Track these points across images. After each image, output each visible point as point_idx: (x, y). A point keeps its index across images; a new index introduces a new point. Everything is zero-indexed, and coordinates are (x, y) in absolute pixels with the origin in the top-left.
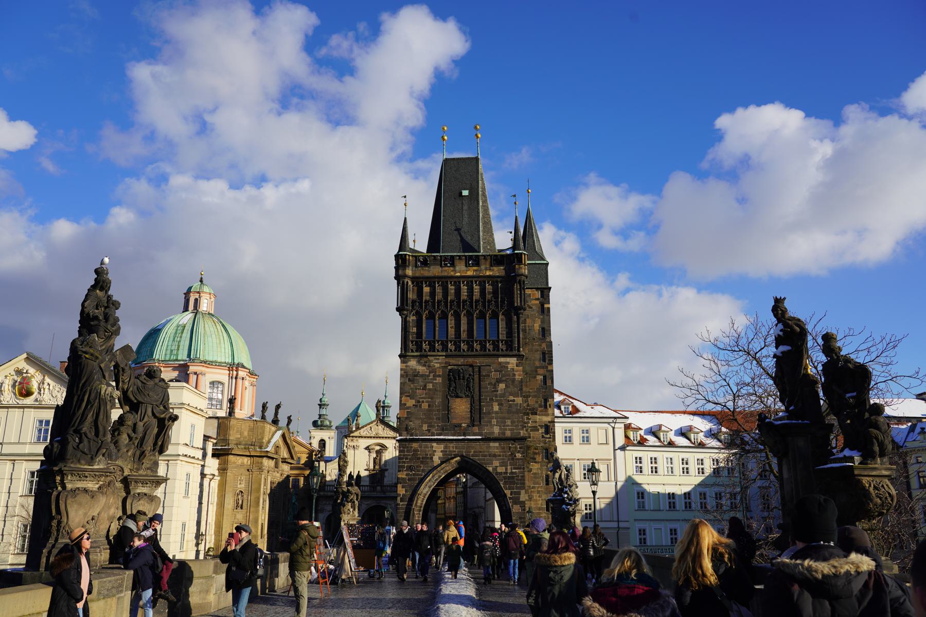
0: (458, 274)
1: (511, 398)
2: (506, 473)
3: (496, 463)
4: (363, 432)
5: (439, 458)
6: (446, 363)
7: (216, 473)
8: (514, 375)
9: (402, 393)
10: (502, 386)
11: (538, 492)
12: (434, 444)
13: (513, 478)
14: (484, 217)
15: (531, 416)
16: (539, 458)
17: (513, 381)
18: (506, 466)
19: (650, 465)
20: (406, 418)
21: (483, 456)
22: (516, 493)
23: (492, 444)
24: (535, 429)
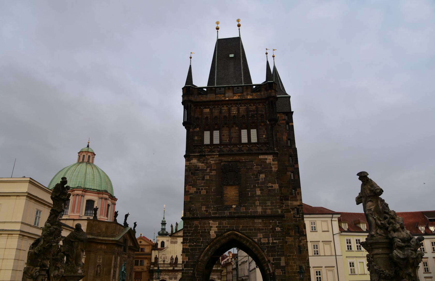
0: (227, 99)
1: (270, 185)
2: (268, 243)
3: (260, 235)
5: (215, 232)
8: (271, 168)
9: (187, 182)
10: (262, 176)
11: (293, 259)
13: (274, 247)
15: (284, 202)
16: (292, 233)
17: (271, 172)
18: (268, 238)
19: (356, 245)
20: (190, 202)
21: (249, 230)
22: (277, 259)
23: (256, 221)
24: (288, 211)
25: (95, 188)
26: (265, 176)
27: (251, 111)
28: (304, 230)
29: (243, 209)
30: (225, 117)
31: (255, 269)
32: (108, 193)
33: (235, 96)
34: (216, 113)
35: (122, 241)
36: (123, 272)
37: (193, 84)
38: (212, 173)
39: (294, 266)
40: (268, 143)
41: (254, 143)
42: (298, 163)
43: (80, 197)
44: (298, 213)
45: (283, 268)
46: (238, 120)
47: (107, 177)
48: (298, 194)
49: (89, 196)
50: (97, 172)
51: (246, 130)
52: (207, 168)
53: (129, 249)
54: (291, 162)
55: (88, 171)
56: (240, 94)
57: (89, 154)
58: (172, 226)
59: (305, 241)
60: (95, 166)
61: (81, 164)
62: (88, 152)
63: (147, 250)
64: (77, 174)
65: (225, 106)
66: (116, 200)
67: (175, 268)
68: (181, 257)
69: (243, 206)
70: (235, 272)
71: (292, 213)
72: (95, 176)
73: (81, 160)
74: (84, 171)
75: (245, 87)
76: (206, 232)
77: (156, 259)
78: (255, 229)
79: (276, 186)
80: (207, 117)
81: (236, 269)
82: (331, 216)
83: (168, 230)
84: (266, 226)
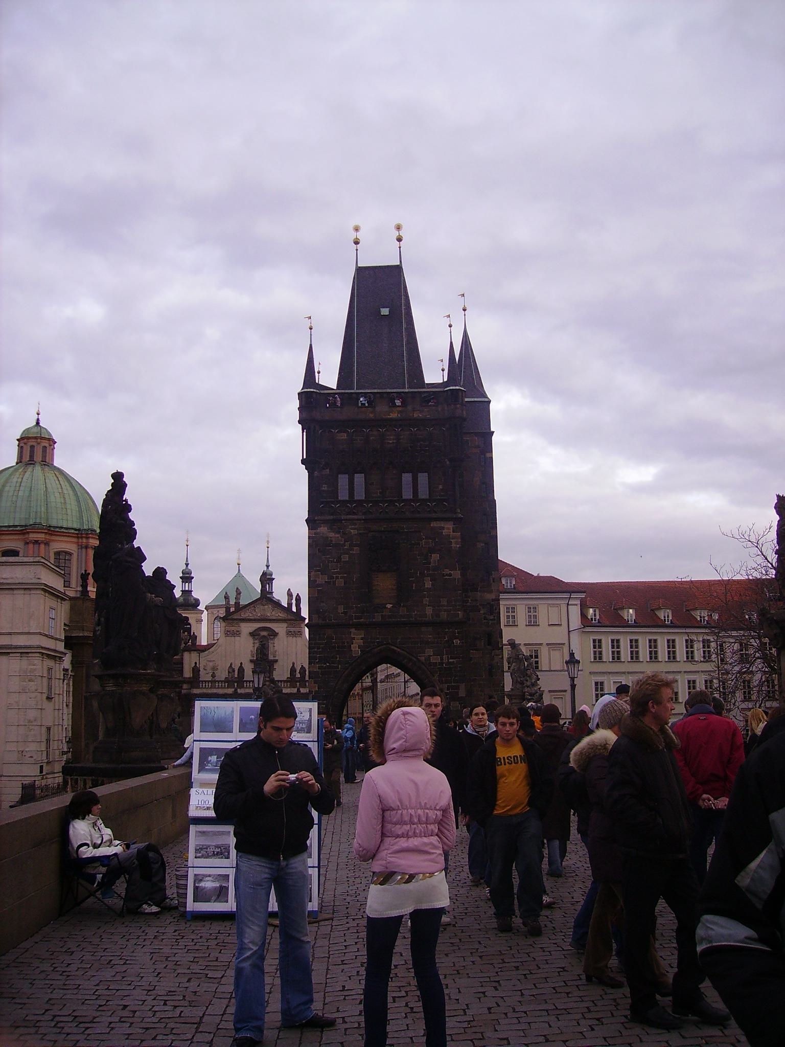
1: (447, 571)
2: (441, 663)
3: (429, 652)
10: (435, 557)
12: (353, 630)
14: (408, 343)
23: (423, 629)
25: (70, 525)
40: (445, 500)
41: (423, 500)
43: (42, 546)
46: (395, 440)
47: (88, 493)
52: (345, 541)
55: (49, 486)
57: (45, 443)
60: (59, 469)
61: (30, 468)
62: (42, 438)
64: (27, 493)
67: (239, 691)
68: (252, 666)
70: (368, 697)
72: (66, 496)
74: (43, 487)
77: (196, 670)
79: (457, 574)
81: (373, 689)
82: (566, 595)
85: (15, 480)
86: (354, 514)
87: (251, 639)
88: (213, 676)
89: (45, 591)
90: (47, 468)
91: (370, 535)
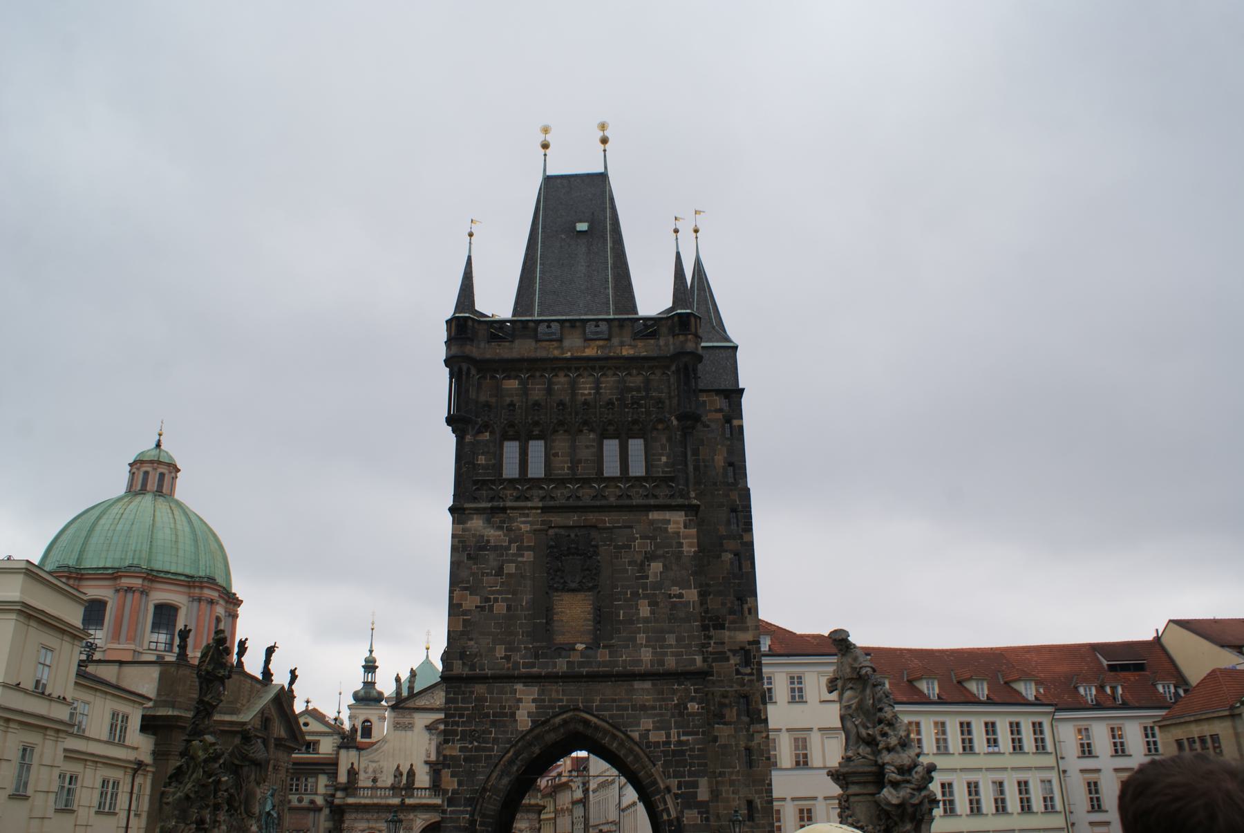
0: (569, 354)
1: (676, 590)
2: (667, 743)
3: (647, 723)
4: (421, 702)
5: (529, 715)
6: (543, 522)
7: (148, 759)
8: (680, 545)
10: (656, 567)
11: (732, 783)
13: (683, 753)
14: (615, 267)
15: (712, 632)
16: (731, 714)
17: (679, 556)
20: (463, 633)
21: (619, 708)
23: (637, 685)
25: (180, 570)
26: (664, 566)
27: (631, 390)
28: (761, 707)
29: (603, 655)
30: (561, 403)
31: (634, 804)
32: (217, 584)
33: (588, 347)
34: (537, 392)
35: (258, 723)
36: (268, 814)
37: (477, 307)
38: (522, 556)
39: (734, 800)
40: (672, 479)
41: (637, 479)
42: (751, 530)
43: (137, 595)
44: (747, 662)
45: (703, 807)
47: (214, 535)
48: (750, 613)
49: (162, 595)
50: (186, 524)
51: (616, 442)
52: (510, 542)
53: (276, 745)
54: (734, 527)
55: (158, 519)
56: (601, 343)
58: (398, 679)
59: (764, 735)
60: (178, 503)
61: (139, 498)
62: (159, 462)
63: (327, 747)
65: (561, 374)
66: (238, 603)
67: (408, 801)
68: (426, 768)
69: (605, 647)
71: (732, 662)
73: (139, 488)
75: (616, 323)
76: (505, 715)
77: (352, 773)
78: (634, 708)
79: (692, 595)
80: (512, 404)
83: (386, 687)
84: (663, 700)
85: (115, 511)
86: (527, 499)
87: (426, 735)
88: (375, 780)
89: (30, 617)
90: (161, 500)
91: (551, 532)
